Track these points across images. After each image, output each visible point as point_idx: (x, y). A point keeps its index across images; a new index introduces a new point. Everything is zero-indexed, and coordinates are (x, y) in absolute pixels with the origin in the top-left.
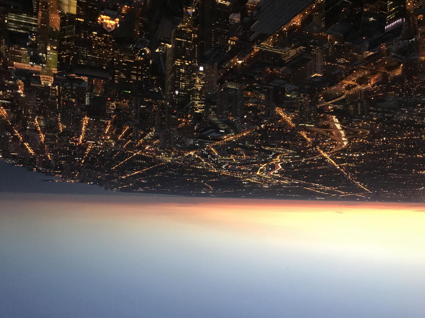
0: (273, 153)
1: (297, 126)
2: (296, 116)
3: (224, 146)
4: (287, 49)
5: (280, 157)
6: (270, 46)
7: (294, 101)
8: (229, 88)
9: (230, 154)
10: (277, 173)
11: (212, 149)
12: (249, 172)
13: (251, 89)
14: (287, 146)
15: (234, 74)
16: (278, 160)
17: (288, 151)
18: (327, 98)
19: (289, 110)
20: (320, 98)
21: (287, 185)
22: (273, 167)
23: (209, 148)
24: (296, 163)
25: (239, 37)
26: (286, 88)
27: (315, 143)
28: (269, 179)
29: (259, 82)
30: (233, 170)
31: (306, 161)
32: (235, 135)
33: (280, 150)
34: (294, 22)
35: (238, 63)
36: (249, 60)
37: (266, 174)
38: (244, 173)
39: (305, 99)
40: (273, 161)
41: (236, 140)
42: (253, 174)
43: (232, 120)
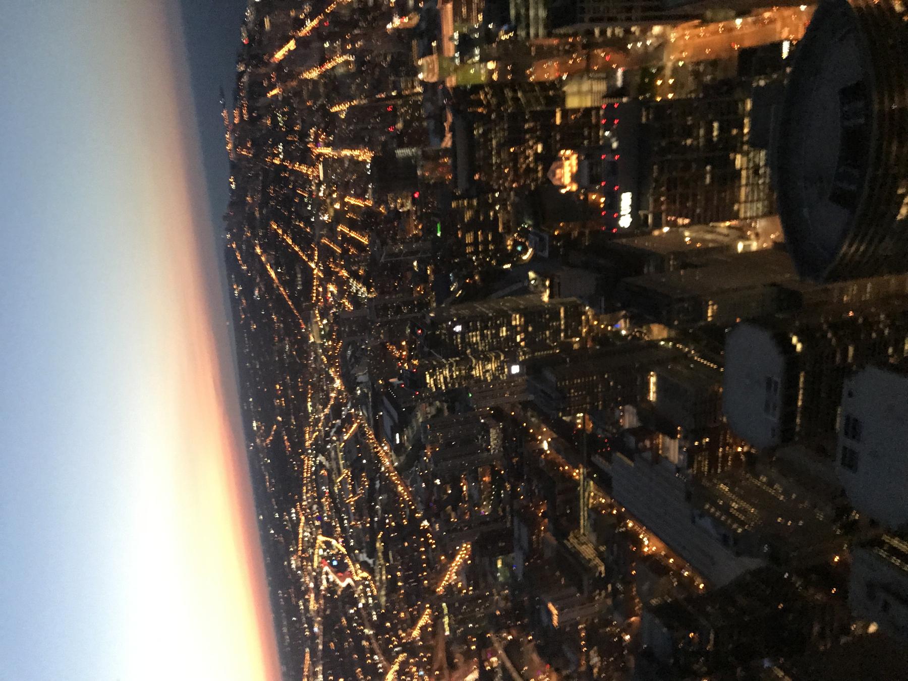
0: (370, 561)
1: (441, 598)
2: (460, 590)
3: (366, 450)
4: (593, 538)
5: (365, 579)
6: (591, 501)
7: (490, 579)
8: (488, 432)
9: (351, 466)
10: (328, 579)
11: (355, 426)
12: (320, 518)
13: (497, 481)
14: (391, 587)
15: (518, 439)
16: (357, 575)
17: (383, 593)
18: (512, 650)
19: (469, 573)
20: (509, 634)
21: (307, 609)
22: (341, 569)
23: (357, 419)
24: (360, 617)
25: (593, 435)
26: (512, 555)
27: (410, 649)
28: (312, 566)
29: (514, 495)
30: (317, 480)
31: (368, 638)
32: (396, 468)
33: (381, 575)
34: (648, 539)
35: (541, 441)
36: (552, 464)
37: (323, 557)
38: (315, 507)
39: (500, 601)
40: (354, 564)
41: (384, 472)
42: (317, 527)
43: (426, 455)
